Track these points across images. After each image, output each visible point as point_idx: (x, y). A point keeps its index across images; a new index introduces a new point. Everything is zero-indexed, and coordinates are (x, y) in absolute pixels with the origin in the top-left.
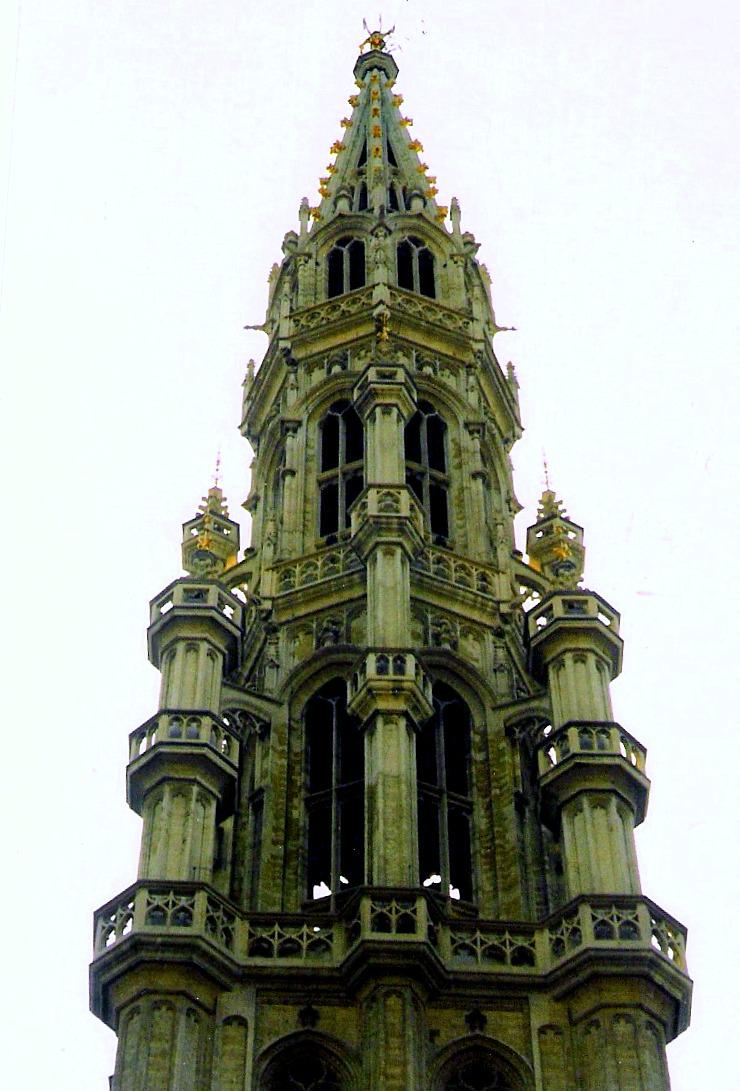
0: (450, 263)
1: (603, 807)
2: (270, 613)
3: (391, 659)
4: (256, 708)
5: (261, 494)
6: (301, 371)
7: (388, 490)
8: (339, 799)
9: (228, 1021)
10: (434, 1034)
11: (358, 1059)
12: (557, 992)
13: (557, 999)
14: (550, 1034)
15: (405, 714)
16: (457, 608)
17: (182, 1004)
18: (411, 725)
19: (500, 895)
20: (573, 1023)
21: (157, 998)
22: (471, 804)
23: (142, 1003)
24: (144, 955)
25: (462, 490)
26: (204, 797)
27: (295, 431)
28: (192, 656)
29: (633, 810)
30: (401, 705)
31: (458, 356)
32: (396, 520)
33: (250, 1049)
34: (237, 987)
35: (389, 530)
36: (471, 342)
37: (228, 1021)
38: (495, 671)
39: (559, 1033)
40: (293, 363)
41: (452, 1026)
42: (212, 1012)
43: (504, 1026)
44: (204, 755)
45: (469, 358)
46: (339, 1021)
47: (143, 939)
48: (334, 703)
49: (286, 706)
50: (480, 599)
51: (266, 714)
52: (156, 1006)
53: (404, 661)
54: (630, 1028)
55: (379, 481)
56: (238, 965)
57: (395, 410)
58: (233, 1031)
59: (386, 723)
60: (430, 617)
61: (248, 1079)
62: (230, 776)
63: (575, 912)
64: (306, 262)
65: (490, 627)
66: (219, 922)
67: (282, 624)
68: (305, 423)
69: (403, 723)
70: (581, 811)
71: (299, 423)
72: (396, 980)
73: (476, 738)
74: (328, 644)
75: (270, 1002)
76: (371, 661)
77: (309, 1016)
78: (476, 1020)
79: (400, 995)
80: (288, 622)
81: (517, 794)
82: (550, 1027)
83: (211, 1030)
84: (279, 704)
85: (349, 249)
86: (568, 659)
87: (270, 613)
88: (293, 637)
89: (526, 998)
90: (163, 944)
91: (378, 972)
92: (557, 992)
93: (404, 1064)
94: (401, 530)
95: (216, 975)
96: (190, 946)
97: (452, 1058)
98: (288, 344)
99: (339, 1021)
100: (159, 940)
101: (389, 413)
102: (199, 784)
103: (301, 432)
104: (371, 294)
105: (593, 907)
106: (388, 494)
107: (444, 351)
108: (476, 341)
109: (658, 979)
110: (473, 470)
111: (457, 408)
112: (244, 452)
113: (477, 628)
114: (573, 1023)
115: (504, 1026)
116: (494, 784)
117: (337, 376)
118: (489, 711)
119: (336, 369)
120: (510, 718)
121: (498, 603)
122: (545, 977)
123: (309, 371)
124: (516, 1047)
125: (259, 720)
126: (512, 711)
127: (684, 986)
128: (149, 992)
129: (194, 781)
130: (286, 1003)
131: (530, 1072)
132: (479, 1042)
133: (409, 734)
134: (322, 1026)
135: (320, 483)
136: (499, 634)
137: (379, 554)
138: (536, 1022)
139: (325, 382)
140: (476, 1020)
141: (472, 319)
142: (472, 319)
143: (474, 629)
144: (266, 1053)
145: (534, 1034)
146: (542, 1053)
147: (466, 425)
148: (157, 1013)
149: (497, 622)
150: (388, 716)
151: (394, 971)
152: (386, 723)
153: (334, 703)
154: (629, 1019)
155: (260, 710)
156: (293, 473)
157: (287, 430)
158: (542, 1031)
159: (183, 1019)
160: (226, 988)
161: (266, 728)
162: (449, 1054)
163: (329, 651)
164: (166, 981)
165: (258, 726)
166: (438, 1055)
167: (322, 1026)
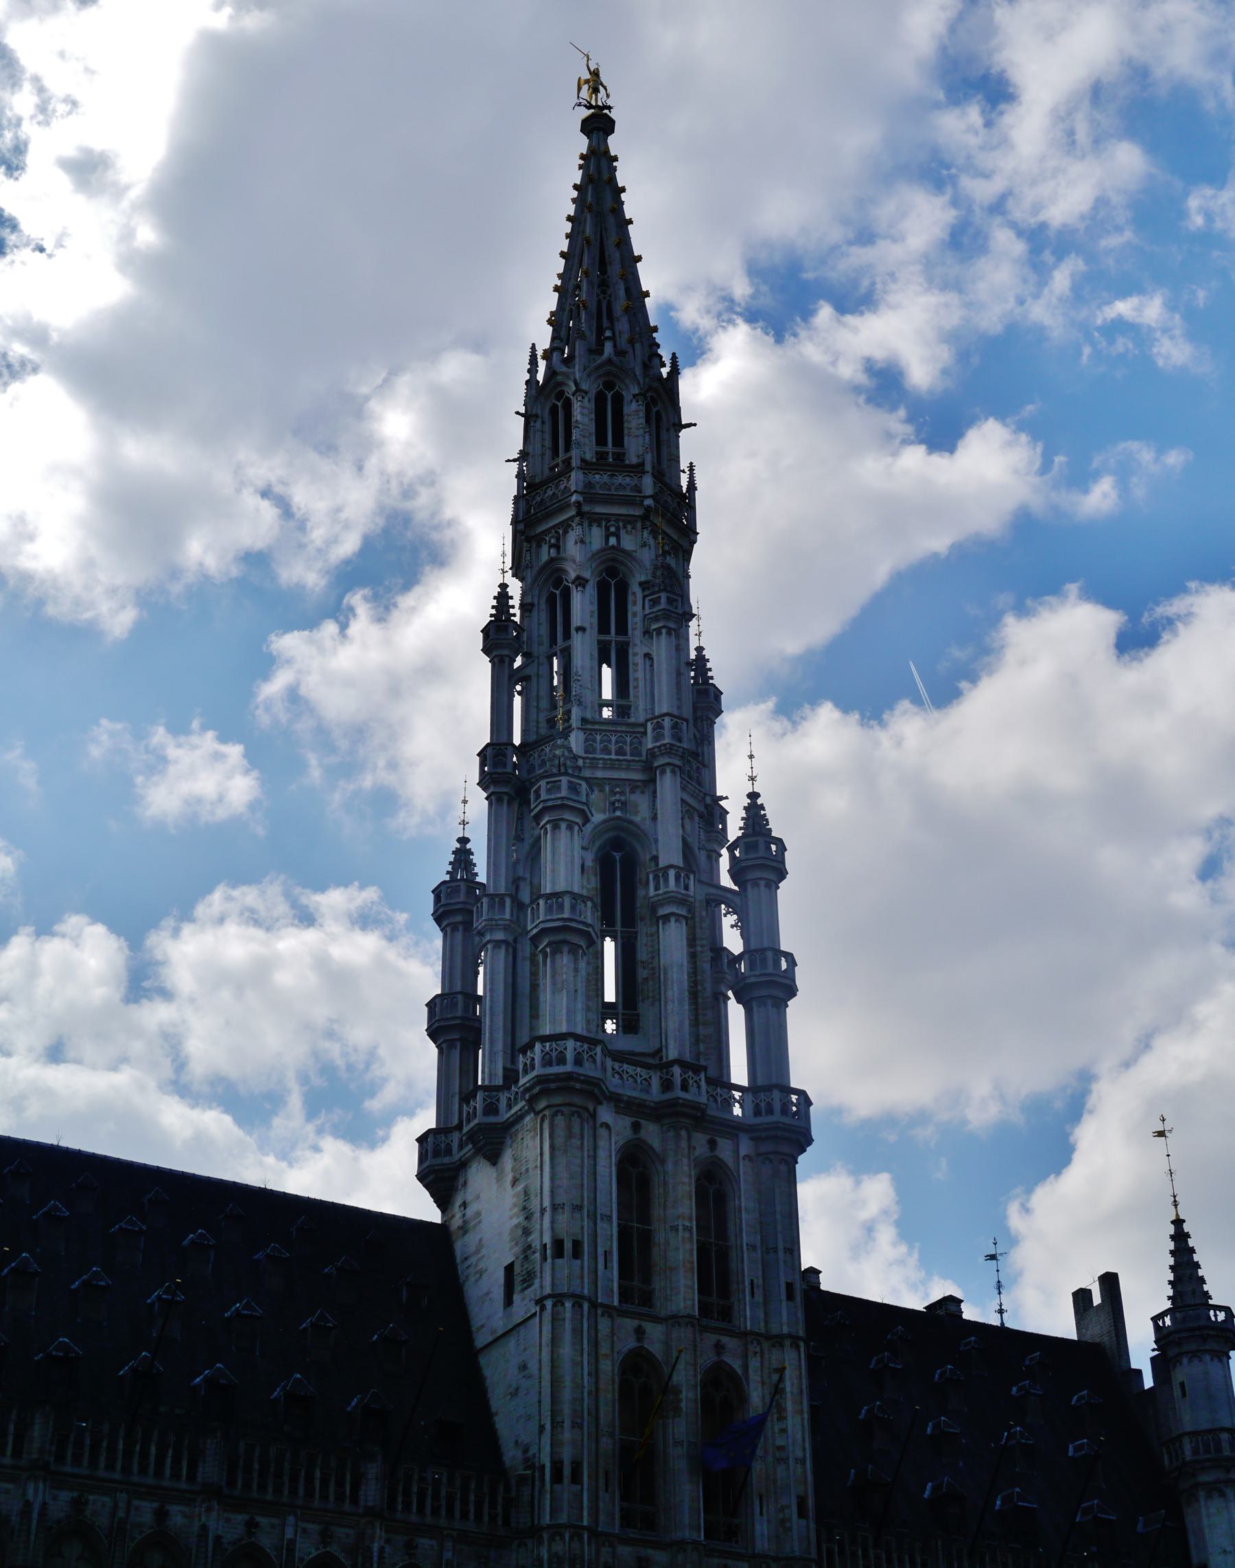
3: (683, 875)
5: (536, 603)
6: (586, 524)
11: (663, 1161)
13: (752, 1139)
14: (747, 1159)
19: (701, 1028)
20: (758, 1155)
21: (574, 1109)
23: (566, 1110)
24: (572, 1083)
30: (684, 912)
31: (680, 541)
32: (681, 750)
33: (613, 1148)
34: (605, 1102)
36: (690, 532)
38: (699, 848)
40: (580, 513)
46: (652, 1133)
47: (574, 1075)
48: (618, 858)
50: (697, 791)
52: (573, 1114)
53: (689, 878)
58: (602, 1132)
64: (583, 398)
65: (697, 811)
72: (687, 1121)
74: (618, 813)
76: (672, 873)
77: (636, 1127)
78: (712, 1144)
85: (612, 396)
89: (737, 1135)
95: (594, 1091)
99: (652, 1133)
100: (582, 1078)
104: (641, 477)
114: (758, 1155)
115: (725, 1150)
116: (698, 942)
117: (613, 547)
119: (613, 541)
120: (710, 894)
121: (705, 794)
122: (750, 1126)
123: (590, 525)
124: (730, 1162)
128: (569, 1104)
130: (626, 1115)
134: (643, 1134)
138: (742, 1153)
139: (602, 550)
140: (712, 1144)
145: (741, 1159)
148: (572, 1118)
153: (618, 858)
160: (600, 1103)
163: (618, 818)
164: (577, 1100)
167: (643, 1134)
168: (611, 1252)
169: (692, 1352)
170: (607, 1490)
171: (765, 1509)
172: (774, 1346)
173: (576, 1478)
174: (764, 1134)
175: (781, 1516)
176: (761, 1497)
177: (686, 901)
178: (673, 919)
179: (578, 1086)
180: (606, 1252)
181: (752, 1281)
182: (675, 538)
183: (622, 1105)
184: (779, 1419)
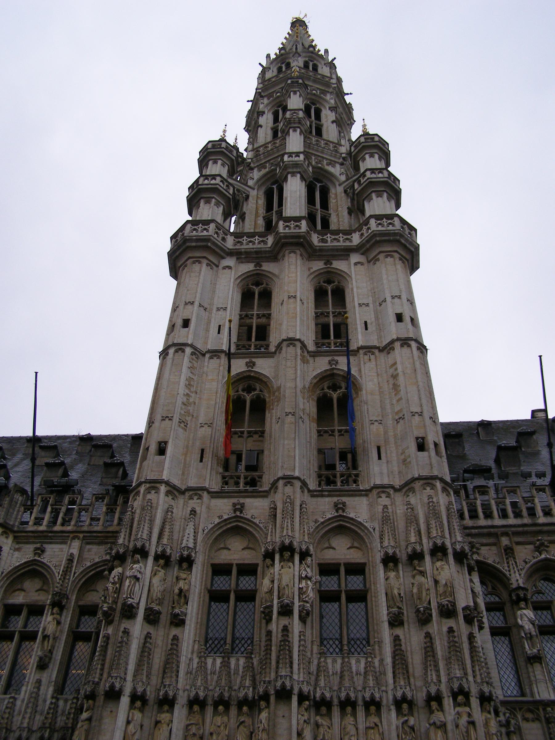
0: (324, 67)
1: (381, 197)
2: (250, 163)
4: (243, 188)
7: (295, 111)
8: (276, 214)
9: (224, 268)
10: (309, 269)
12: (361, 251)
13: (362, 254)
15: (299, 173)
16: (324, 156)
17: (205, 262)
18: (302, 178)
20: (369, 262)
22: (330, 214)
25: (328, 127)
26: (217, 204)
27: (262, 115)
28: (215, 165)
29: (393, 199)
33: (233, 276)
35: (295, 123)
37: (224, 268)
39: (362, 264)
41: (318, 265)
42: (217, 266)
43: (339, 265)
44: (217, 188)
45: (331, 90)
49: (256, 191)
51: (247, 191)
52: (194, 263)
54: (392, 259)
55: (291, 108)
56: (228, 249)
57: (298, 92)
58: (227, 271)
59: (292, 176)
60: (313, 158)
61: (232, 285)
62: (229, 198)
63: (369, 222)
65: (338, 163)
66: (220, 235)
67: (255, 167)
68: (266, 112)
69: (299, 175)
70: (372, 199)
71: (264, 112)
73: (333, 196)
75: (242, 262)
79: (295, 253)
80: (257, 166)
81: (348, 208)
82: (359, 263)
83: (217, 272)
84: (254, 189)
86: (367, 156)
87: (250, 163)
88: (260, 170)
89: (349, 255)
90: (196, 239)
91: (284, 245)
92: (361, 251)
93: (296, 272)
94: (300, 123)
96: (207, 239)
97: (316, 276)
98: (260, 91)
100: (194, 238)
101: (296, 94)
102: (216, 199)
103: (265, 116)
105: (376, 219)
106: (295, 113)
107: (321, 88)
108: (334, 84)
109: (403, 241)
110: (332, 120)
111: (325, 104)
112: (246, 136)
113: (333, 163)
114: (369, 262)
115: (339, 265)
118: (337, 186)
120: (345, 186)
121: (341, 154)
125: (245, 193)
126: (346, 184)
127: (417, 248)
129: (213, 198)
130: (249, 262)
131: (350, 276)
132: (329, 270)
133: (302, 181)
135: (272, 129)
136: (342, 164)
137: (291, 131)
141: (332, 78)
142: (332, 78)
143: (332, 163)
144: (239, 277)
146: (355, 271)
147: (330, 108)
149: (341, 160)
150: (293, 174)
151: (292, 244)
152: (292, 176)
154: (392, 256)
155: (245, 189)
156: (261, 126)
157: (259, 115)
158: (356, 264)
159: (204, 265)
160: (223, 258)
161: (247, 197)
162: (317, 273)
164: (198, 254)
165: (244, 195)
166: (311, 274)
168: (224, 325)
169: (294, 361)
170: (201, 461)
171: (383, 455)
172: (389, 353)
173: (162, 451)
174: (368, 246)
175: (403, 457)
176: (379, 448)
177: (298, 164)
178: (289, 176)
179: (194, 244)
180: (220, 326)
181: (366, 323)
182: (323, 89)
183: (243, 256)
184: (396, 395)
